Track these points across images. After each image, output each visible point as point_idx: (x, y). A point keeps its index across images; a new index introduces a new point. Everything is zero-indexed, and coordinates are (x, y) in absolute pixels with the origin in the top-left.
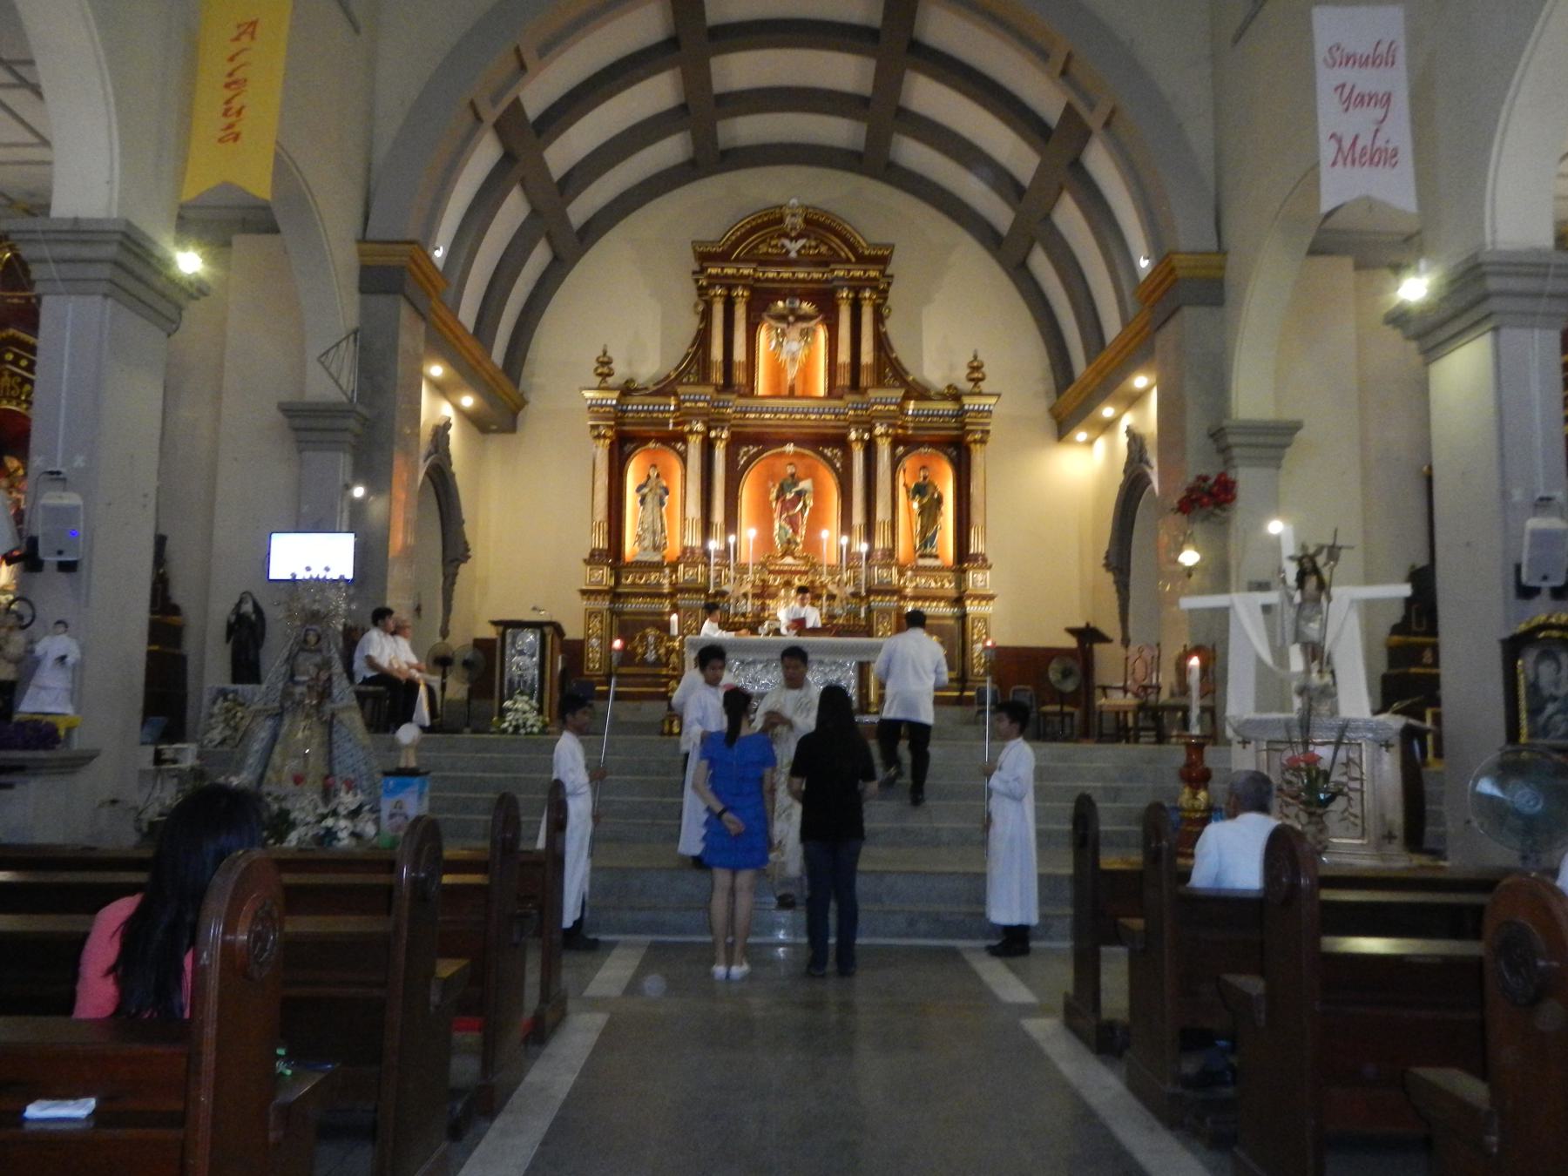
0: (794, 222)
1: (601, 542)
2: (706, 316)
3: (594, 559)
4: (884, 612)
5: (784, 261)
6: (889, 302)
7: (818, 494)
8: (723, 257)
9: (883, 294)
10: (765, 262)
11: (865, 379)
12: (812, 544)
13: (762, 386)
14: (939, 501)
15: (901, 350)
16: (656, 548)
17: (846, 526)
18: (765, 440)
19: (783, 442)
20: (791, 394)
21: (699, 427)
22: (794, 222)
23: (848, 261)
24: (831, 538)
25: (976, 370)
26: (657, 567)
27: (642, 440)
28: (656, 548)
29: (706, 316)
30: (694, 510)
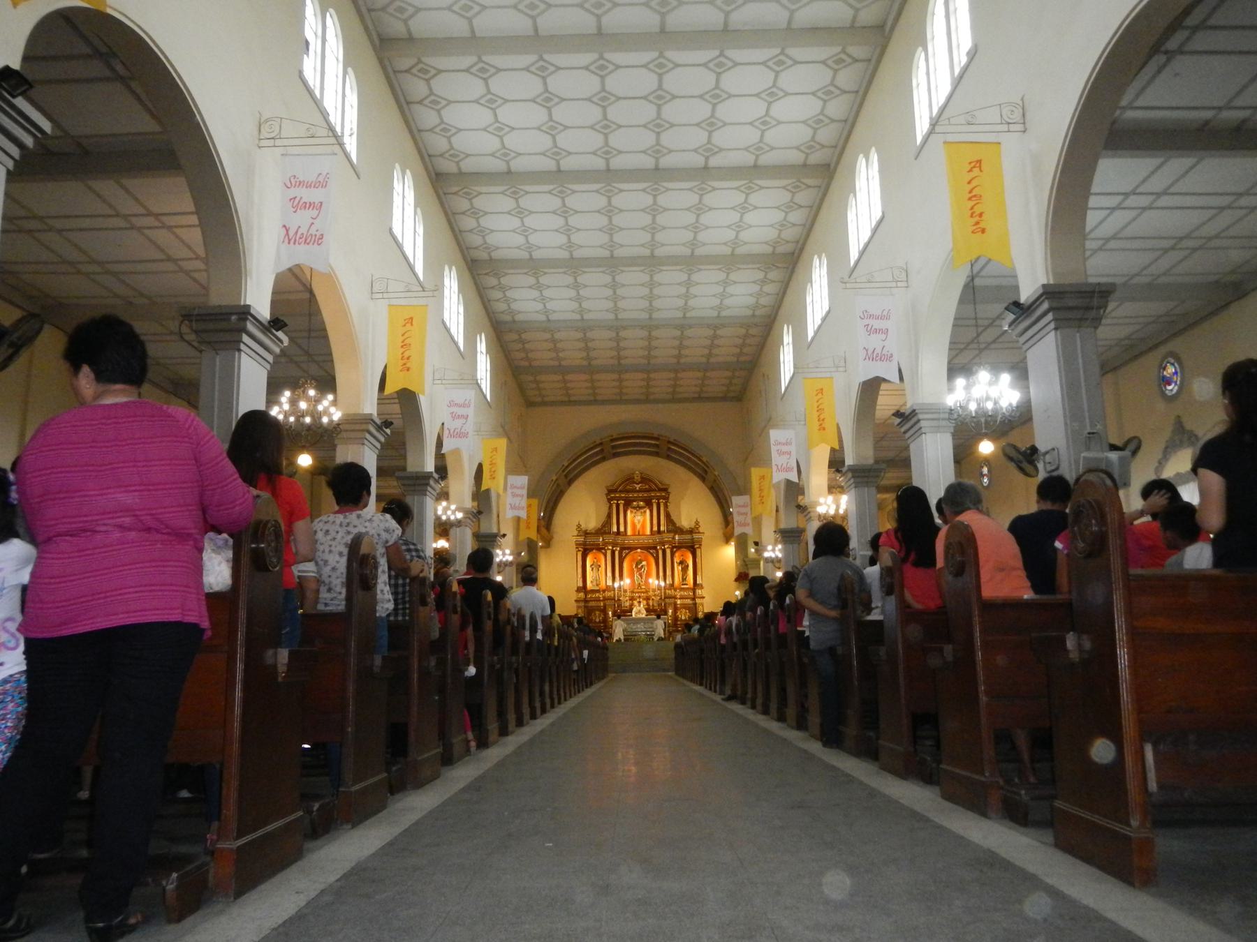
0: (637, 478)
1: (580, 584)
2: (610, 507)
3: (579, 590)
4: (670, 604)
5: (634, 491)
6: (670, 500)
7: (648, 565)
8: (615, 491)
9: (666, 498)
10: (628, 491)
11: (662, 528)
12: (647, 583)
13: (629, 532)
14: (688, 566)
15: (674, 517)
16: (597, 585)
17: (658, 577)
18: (631, 549)
19: (636, 548)
20: (639, 535)
21: (610, 548)
22: (637, 478)
23: (654, 490)
24: (654, 582)
25: (697, 523)
26: (598, 591)
27: (592, 550)
28: (597, 585)
29: (610, 507)
30: (609, 574)
